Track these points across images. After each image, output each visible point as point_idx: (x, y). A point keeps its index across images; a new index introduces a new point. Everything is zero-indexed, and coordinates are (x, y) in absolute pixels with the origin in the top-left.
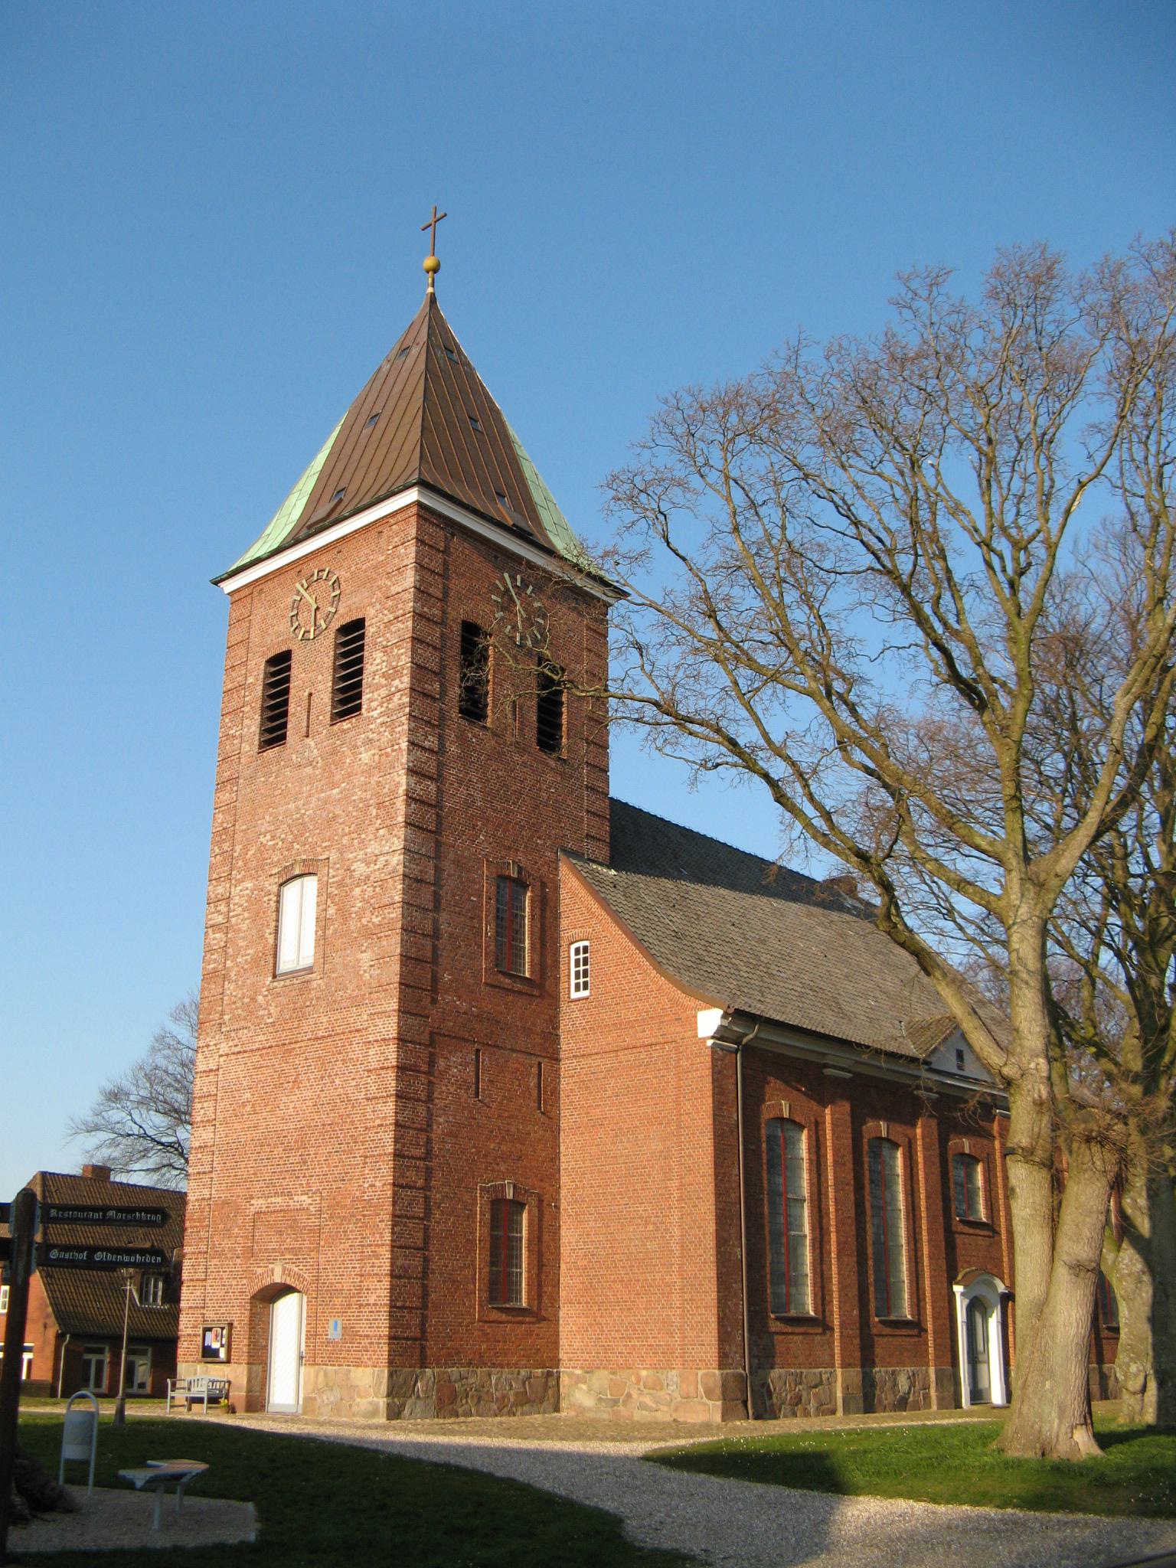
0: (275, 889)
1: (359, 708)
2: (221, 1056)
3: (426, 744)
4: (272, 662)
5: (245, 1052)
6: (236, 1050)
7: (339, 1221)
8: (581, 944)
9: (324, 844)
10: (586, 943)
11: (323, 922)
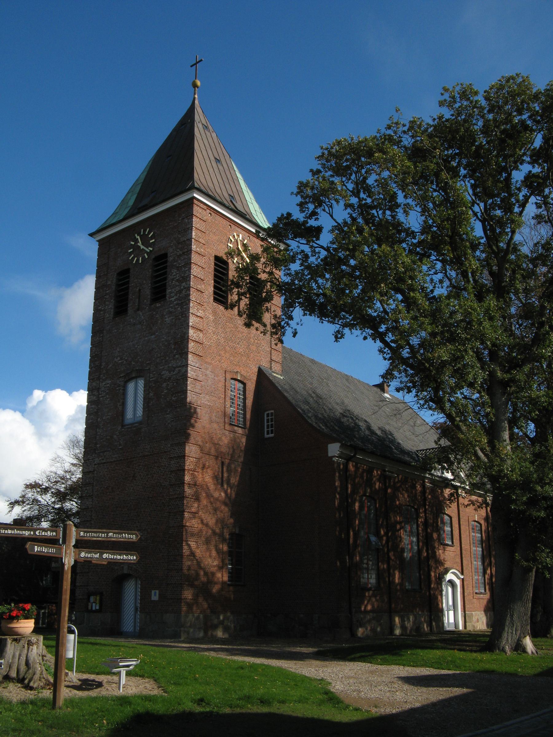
0: (122, 384)
1: (165, 296)
2: (95, 464)
3: (199, 314)
4: (120, 274)
5: (108, 462)
6: (104, 461)
8: (270, 412)
9: (147, 362)
10: (272, 411)
11: (147, 400)
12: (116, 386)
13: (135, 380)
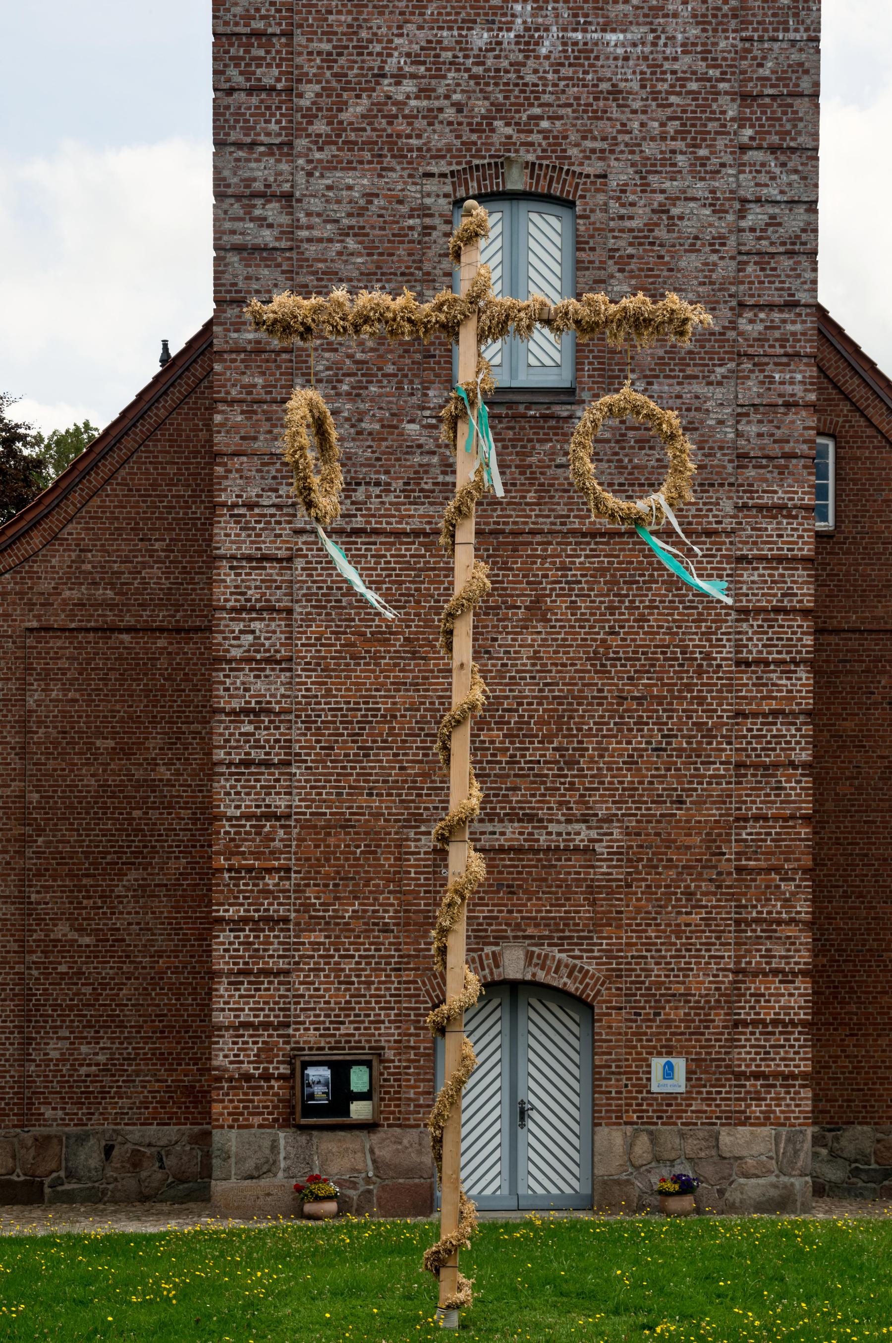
5: (376, 532)
6: (359, 522)
7: (672, 873)
9: (589, 144)
12: (404, 209)
13: (505, 206)
